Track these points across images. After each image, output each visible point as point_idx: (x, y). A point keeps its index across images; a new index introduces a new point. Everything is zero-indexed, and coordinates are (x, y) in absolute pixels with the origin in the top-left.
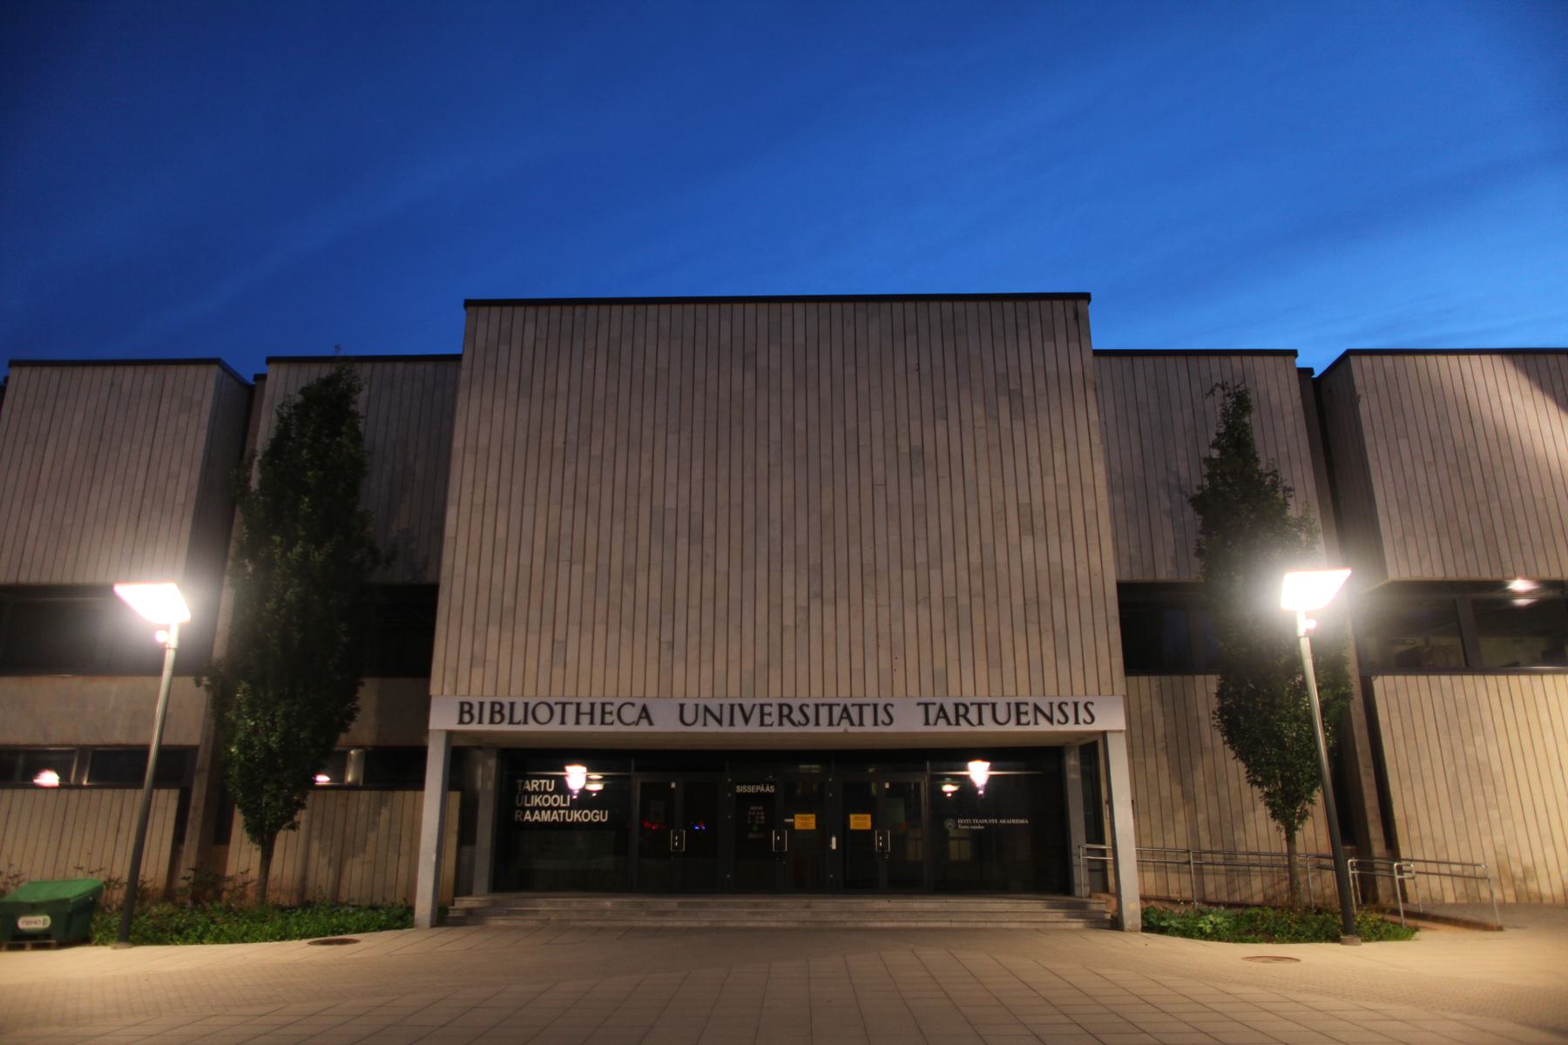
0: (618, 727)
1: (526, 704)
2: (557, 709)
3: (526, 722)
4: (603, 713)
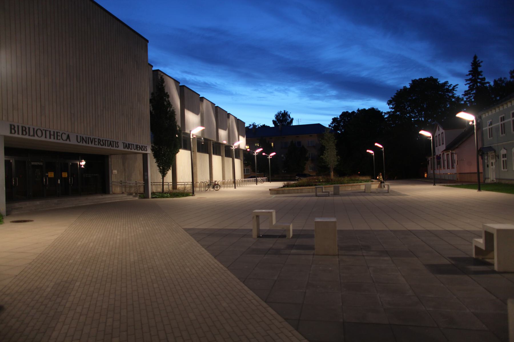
0: (61, 141)
1: (34, 129)
2: (44, 132)
3: (34, 136)
4: (57, 136)
